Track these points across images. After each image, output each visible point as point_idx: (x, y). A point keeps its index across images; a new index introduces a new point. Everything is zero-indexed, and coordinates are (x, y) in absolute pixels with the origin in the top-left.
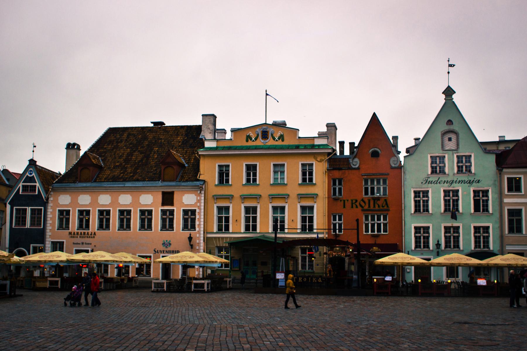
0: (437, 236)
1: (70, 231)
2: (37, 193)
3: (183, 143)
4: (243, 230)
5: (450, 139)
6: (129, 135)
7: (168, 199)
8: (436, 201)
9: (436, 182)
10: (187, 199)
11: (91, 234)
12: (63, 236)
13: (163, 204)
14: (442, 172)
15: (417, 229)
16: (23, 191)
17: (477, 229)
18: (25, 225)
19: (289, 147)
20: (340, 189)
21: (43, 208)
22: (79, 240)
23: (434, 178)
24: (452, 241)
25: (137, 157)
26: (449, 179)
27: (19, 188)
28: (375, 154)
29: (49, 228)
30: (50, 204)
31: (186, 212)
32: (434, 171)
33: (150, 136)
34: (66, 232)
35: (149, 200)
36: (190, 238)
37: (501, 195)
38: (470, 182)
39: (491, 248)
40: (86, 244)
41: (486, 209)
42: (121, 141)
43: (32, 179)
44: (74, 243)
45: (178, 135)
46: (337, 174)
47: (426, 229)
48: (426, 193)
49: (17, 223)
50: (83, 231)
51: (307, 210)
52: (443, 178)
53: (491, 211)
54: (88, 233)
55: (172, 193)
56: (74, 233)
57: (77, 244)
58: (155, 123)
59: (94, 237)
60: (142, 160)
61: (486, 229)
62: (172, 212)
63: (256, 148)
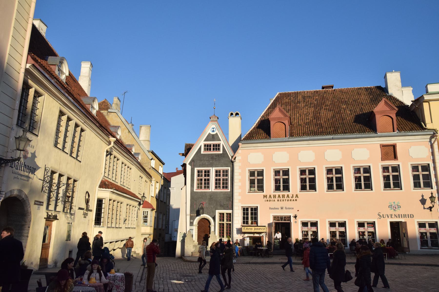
1: (264, 193)
2: (221, 152)
6: (304, 97)
7: (390, 152)
11: (292, 197)
12: (255, 199)
13: (383, 159)
16: (205, 149)
18: (208, 187)
21: (229, 168)
27: (201, 147)
40: (286, 208)
42: (299, 102)
44: (270, 208)
49: (199, 187)
50: (281, 193)
54: (288, 196)
56: (270, 196)
57: (275, 209)
59: (296, 200)
60: (334, 116)
62: (396, 169)
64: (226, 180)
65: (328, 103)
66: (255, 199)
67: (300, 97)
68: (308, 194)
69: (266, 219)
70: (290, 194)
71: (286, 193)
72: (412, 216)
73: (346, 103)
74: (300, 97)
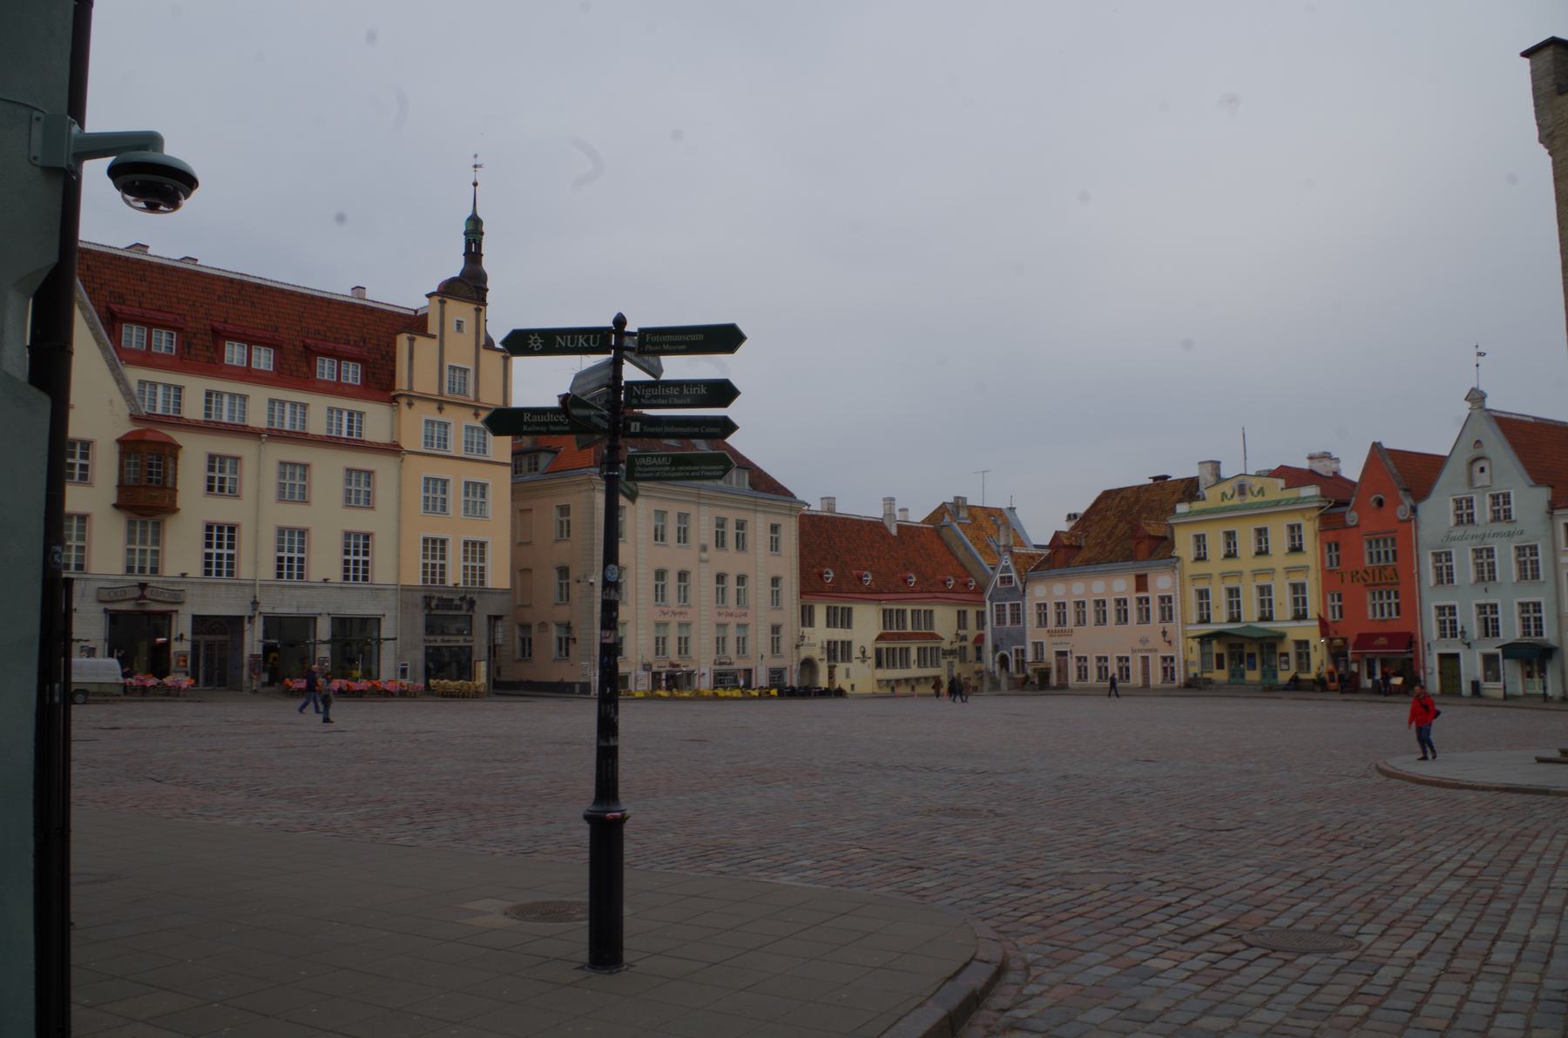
0: (1469, 620)
4: (1225, 618)
5: (1482, 470)
7: (1141, 583)
8: (1464, 567)
9: (1461, 538)
10: (1161, 582)
13: (1138, 589)
14: (1471, 520)
15: (1441, 609)
17: (1524, 606)
22: (1056, 639)
23: (1459, 531)
24: (1490, 627)
26: (1479, 532)
28: (1380, 503)
29: (1028, 625)
30: (1027, 598)
31: (1162, 599)
32: (1460, 522)
35: (1121, 585)
36: (1164, 633)
37: (1555, 550)
38: (1509, 535)
39: (1545, 636)
41: (1536, 576)
43: (1006, 569)
46: (1331, 536)
47: (1452, 608)
48: (1448, 554)
51: (1298, 588)
52: (1471, 531)
53: (1542, 578)
55: (1145, 576)
58: (1155, 479)
61: (1537, 606)
62: (1147, 600)
63: (1232, 509)
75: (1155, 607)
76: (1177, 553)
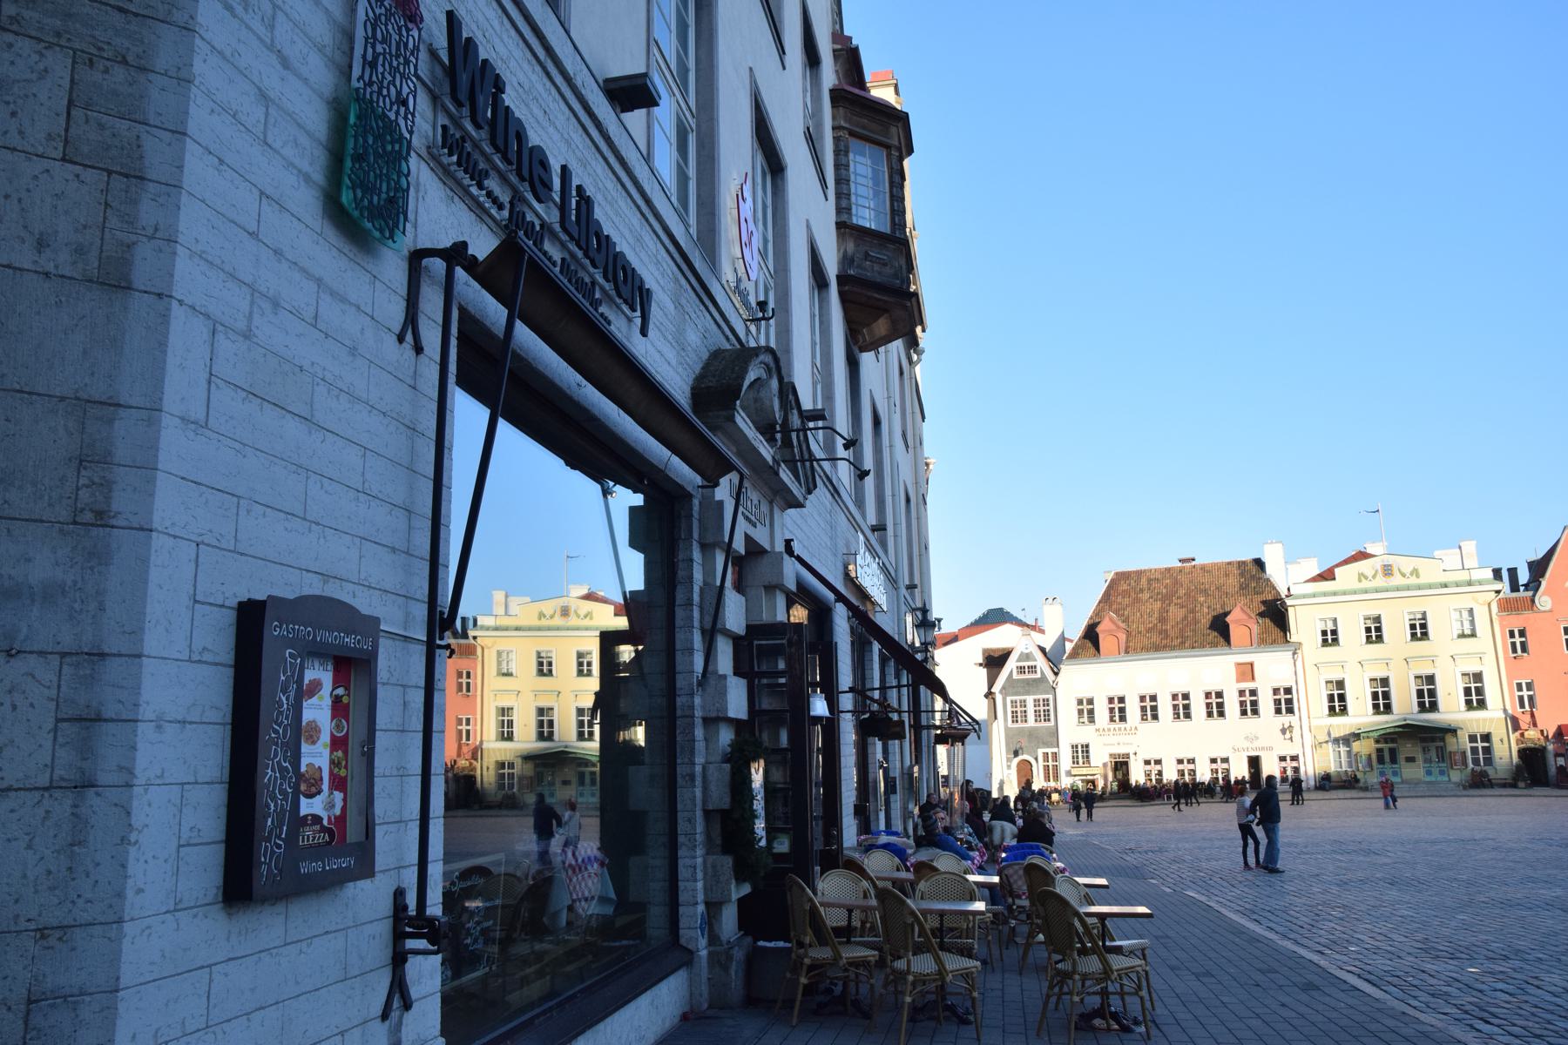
3: (1241, 588)
6: (1149, 580)
7: (1247, 671)
12: (1085, 734)
19: (1430, 587)
20: (1523, 644)
25: (1175, 613)
33: (1183, 579)
34: (1091, 728)
42: (1142, 591)
45: (1227, 575)
60: (1185, 618)
62: (1253, 693)
64: (1046, 712)
65: (1182, 592)
66: (1085, 734)
67: (1144, 581)
68: (1151, 725)
69: (1100, 758)
70: (1128, 726)
71: (1122, 725)
72: (1271, 749)
73: (1205, 592)
74: (1144, 581)
75: (1266, 703)
76: (1294, 636)
